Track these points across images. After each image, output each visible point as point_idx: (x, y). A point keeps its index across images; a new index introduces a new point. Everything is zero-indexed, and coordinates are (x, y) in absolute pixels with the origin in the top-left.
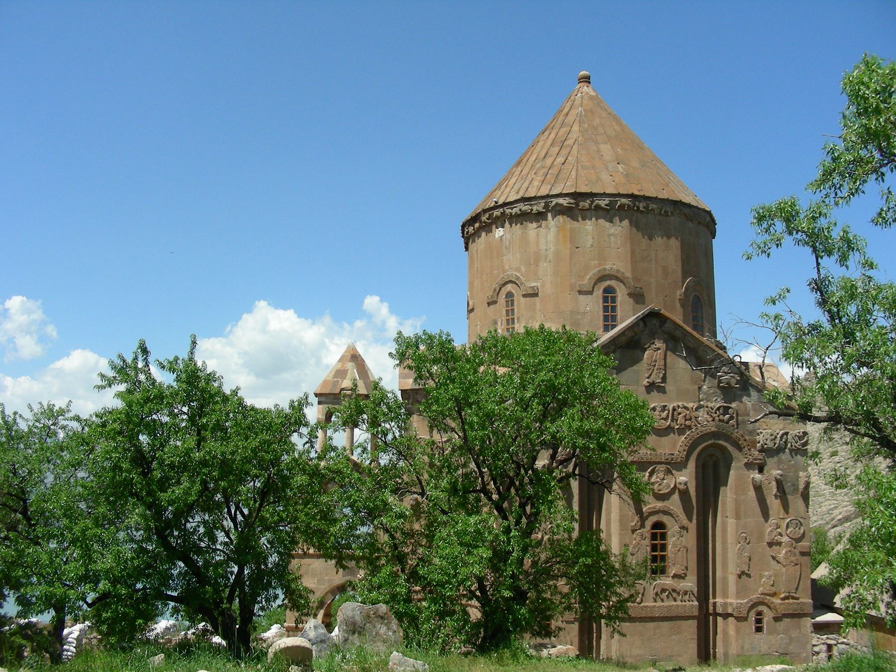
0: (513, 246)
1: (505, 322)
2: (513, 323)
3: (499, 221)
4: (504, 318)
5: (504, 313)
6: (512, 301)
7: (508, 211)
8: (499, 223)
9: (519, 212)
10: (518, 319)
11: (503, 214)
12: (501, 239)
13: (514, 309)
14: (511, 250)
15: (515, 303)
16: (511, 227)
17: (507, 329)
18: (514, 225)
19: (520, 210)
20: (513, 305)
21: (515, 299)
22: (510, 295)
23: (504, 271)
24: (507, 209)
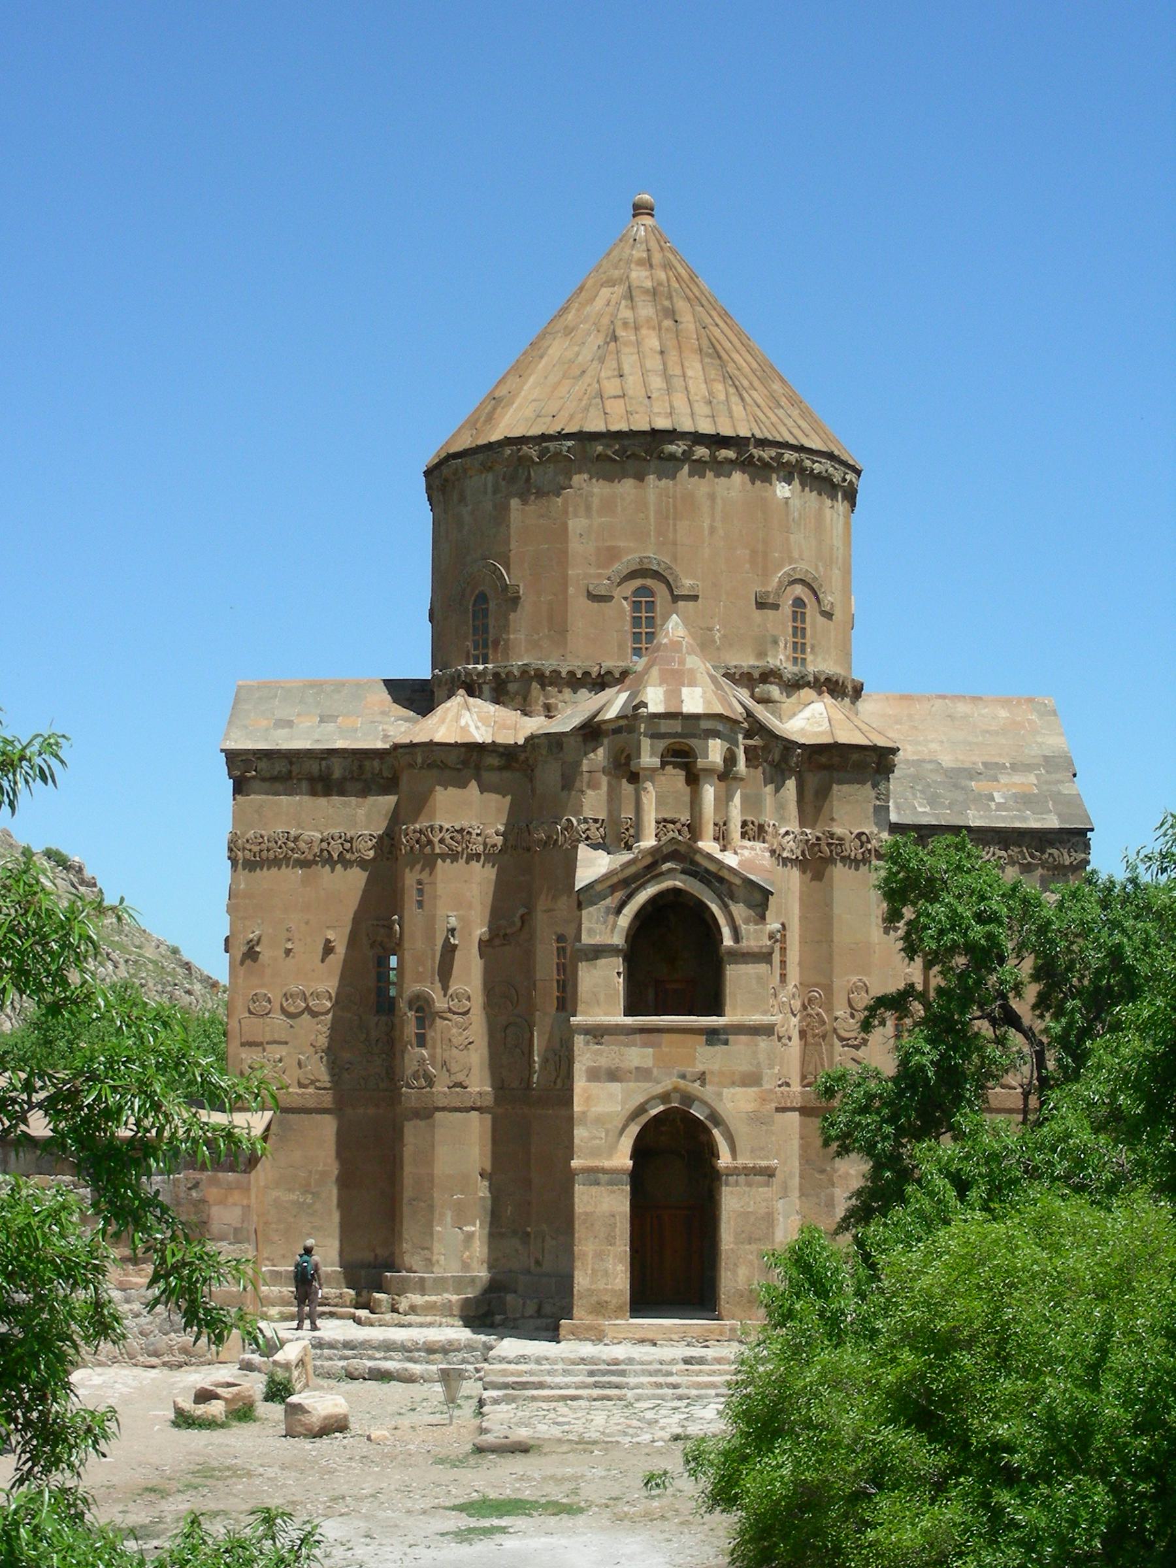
0: (805, 524)
1: (790, 645)
2: (803, 651)
3: (790, 472)
4: (790, 639)
5: (790, 630)
6: (803, 614)
7: (808, 463)
8: (782, 474)
9: (824, 474)
10: (813, 648)
11: (799, 462)
12: (787, 503)
13: (805, 629)
14: (802, 527)
15: (808, 619)
16: (803, 490)
17: (794, 658)
18: (807, 489)
19: (826, 471)
20: (803, 621)
21: (808, 611)
22: (799, 602)
23: (791, 560)
24: (807, 458)
